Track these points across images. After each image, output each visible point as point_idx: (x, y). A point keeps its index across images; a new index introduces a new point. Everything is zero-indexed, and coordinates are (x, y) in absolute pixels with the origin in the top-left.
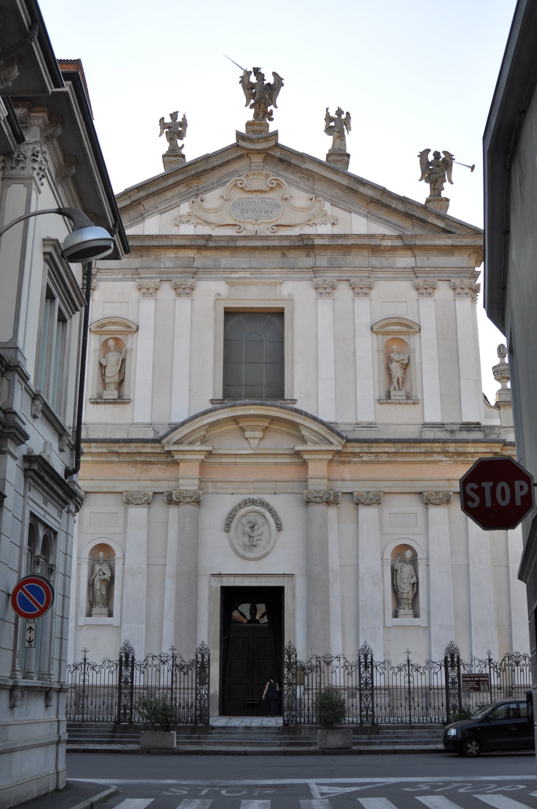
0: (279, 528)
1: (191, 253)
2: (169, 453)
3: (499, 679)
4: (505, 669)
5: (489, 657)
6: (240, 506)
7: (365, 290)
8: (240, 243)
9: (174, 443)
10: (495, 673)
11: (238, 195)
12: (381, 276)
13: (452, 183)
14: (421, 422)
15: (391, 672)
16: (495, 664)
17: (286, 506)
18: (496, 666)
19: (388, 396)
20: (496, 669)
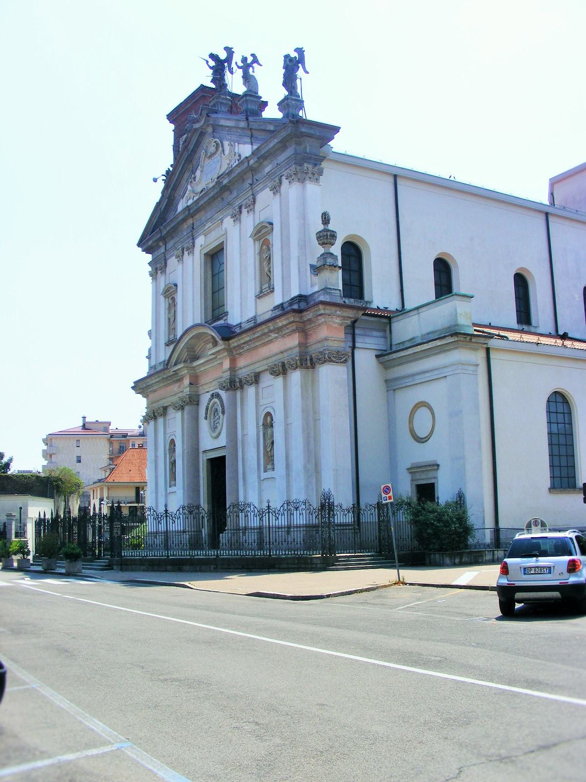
0: (223, 413)
1: (190, 221)
2: (176, 373)
3: (174, 525)
4: (230, 516)
5: (269, 505)
6: (210, 400)
7: (252, 207)
8: (201, 203)
9: (174, 366)
10: (171, 521)
11: (207, 161)
12: (258, 189)
13: (307, 73)
14: (272, 308)
15: (342, 513)
16: (171, 514)
17: (223, 394)
18: (172, 515)
19: (261, 292)
20: (171, 518)
